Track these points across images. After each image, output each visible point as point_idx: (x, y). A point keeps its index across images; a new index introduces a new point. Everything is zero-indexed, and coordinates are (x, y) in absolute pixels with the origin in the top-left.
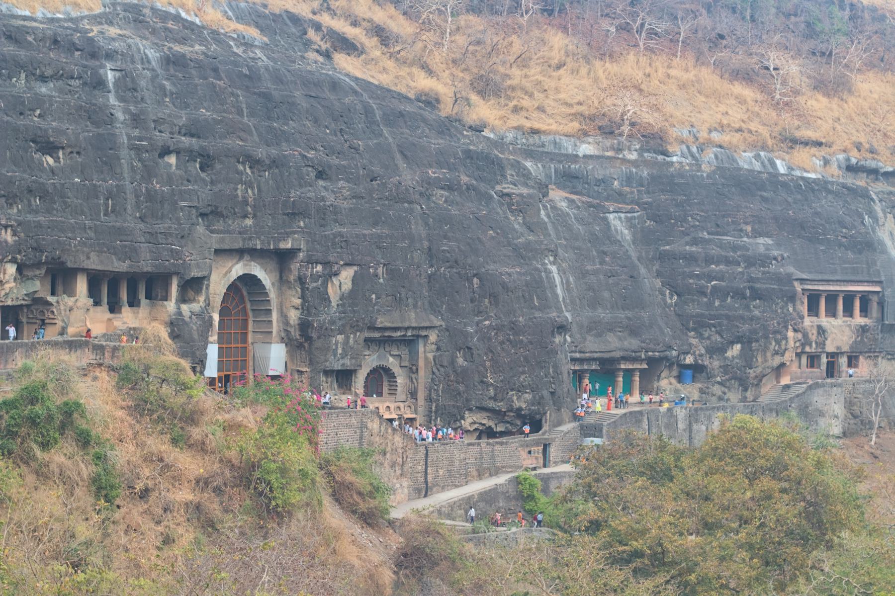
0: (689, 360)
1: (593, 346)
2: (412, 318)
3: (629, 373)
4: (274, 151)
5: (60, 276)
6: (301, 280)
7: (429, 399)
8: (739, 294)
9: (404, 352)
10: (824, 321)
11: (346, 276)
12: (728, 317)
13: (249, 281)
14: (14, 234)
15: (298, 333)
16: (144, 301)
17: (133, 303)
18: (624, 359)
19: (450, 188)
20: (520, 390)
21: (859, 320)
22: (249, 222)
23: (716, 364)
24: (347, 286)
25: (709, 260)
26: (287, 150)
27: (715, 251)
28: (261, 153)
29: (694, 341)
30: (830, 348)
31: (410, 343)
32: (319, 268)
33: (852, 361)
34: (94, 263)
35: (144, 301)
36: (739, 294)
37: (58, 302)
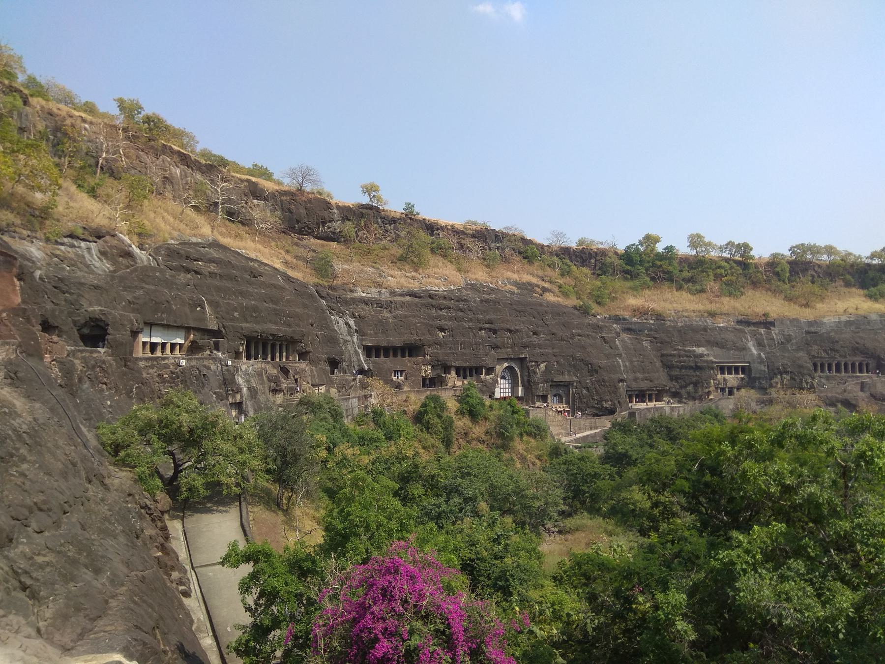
0: (673, 390)
1: (634, 385)
2: (567, 378)
4: (517, 327)
5: (447, 369)
10: (727, 376)
17: (471, 375)
20: (606, 401)
27: (682, 353)
30: (729, 385)
34: (457, 364)
36: (691, 368)
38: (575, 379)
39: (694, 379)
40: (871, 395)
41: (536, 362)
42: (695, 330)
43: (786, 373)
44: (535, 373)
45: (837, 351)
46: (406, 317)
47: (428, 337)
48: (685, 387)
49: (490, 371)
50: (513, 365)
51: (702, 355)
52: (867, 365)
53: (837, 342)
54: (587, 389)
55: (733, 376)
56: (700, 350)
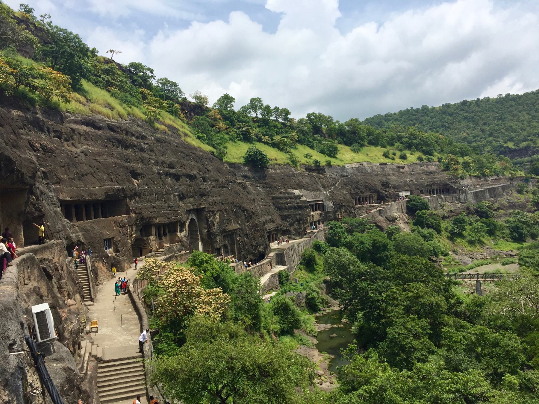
0: (285, 228)
7: (239, 253)
8: (295, 208)
10: (312, 213)
12: (293, 214)
14: (135, 213)
16: (168, 234)
17: (165, 235)
19: (231, 182)
20: (260, 246)
22: (192, 199)
25: (286, 198)
26: (193, 172)
27: (287, 195)
28: (192, 173)
29: (286, 223)
30: (315, 220)
34: (157, 221)
35: (168, 234)
36: (295, 208)
37: (147, 239)
38: (239, 226)
39: (298, 217)
40: (386, 218)
41: (213, 212)
42: (288, 176)
45: (359, 189)
46: (99, 154)
49: (183, 225)
50: (195, 217)
51: (299, 197)
52: (372, 197)
53: (358, 182)
54: (247, 235)
55: (315, 213)
56: (297, 192)
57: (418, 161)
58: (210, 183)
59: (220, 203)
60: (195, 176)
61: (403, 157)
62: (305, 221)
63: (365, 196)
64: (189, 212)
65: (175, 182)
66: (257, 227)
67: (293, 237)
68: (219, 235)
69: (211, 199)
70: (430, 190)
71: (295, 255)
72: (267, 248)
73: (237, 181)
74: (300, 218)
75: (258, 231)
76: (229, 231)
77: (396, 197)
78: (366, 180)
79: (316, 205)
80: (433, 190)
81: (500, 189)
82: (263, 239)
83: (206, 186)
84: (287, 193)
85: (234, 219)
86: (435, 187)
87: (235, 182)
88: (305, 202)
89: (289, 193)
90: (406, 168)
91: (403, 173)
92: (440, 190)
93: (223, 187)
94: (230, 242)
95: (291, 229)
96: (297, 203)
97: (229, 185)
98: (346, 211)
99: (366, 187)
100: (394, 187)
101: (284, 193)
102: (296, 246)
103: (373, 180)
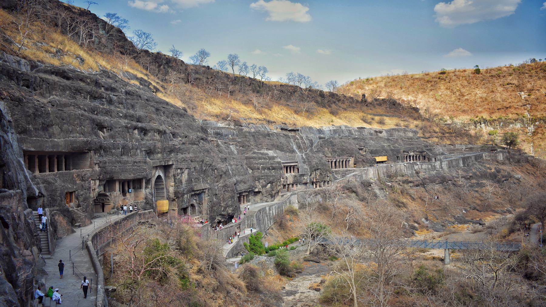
0: (257, 190)
3: (244, 196)
6: (174, 176)
8: (269, 169)
9: (197, 198)
11: (186, 172)
13: (159, 177)
14: (99, 167)
15: (173, 196)
18: (245, 192)
19: (202, 139)
21: (293, 174)
23: (264, 190)
24: (187, 177)
27: (260, 156)
29: (258, 184)
30: (288, 183)
31: (199, 194)
32: (179, 170)
33: (293, 185)
37: (110, 195)
41: (181, 169)
43: (318, 169)
44: (181, 182)
47: (94, 138)
48: (266, 186)
49: (148, 181)
51: (273, 158)
56: (271, 153)
57: (396, 127)
58: (180, 139)
59: (189, 161)
60: (165, 131)
61: (381, 123)
62: (278, 184)
63: (341, 160)
64: (156, 167)
65: (143, 136)
66: (228, 188)
67: (265, 199)
68: (187, 194)
69: (180, 156)
70: (407, 157)
71: (266, 218)
72: (237, 209)
73: (209, 139)
74: (274, 180)
75: (228, 191)
76: (198, 190)
77: (373, 163)
78: (343, 143)
79: (290, 167)
80: (410, 156)
81: (473, 158)
82: (233, 200)
83: (177, 142)
84: (261, 153)
85: (203, 178)
86: (412, 154)
87: (206, 139)
88: (279, 163)
89: (262, 154)
90: (384, 134)
91: (381, 138)
92: (416, 157)
93: (195, 144)
94: (198, 202)
95: (263, 191)
96: (271, 164)
97: (199, 142)
98: (321, 174)
99: (343, 150)
100: (372, 152)
101: (258, 153)
102: (267, 209)
103: (350, 144)
